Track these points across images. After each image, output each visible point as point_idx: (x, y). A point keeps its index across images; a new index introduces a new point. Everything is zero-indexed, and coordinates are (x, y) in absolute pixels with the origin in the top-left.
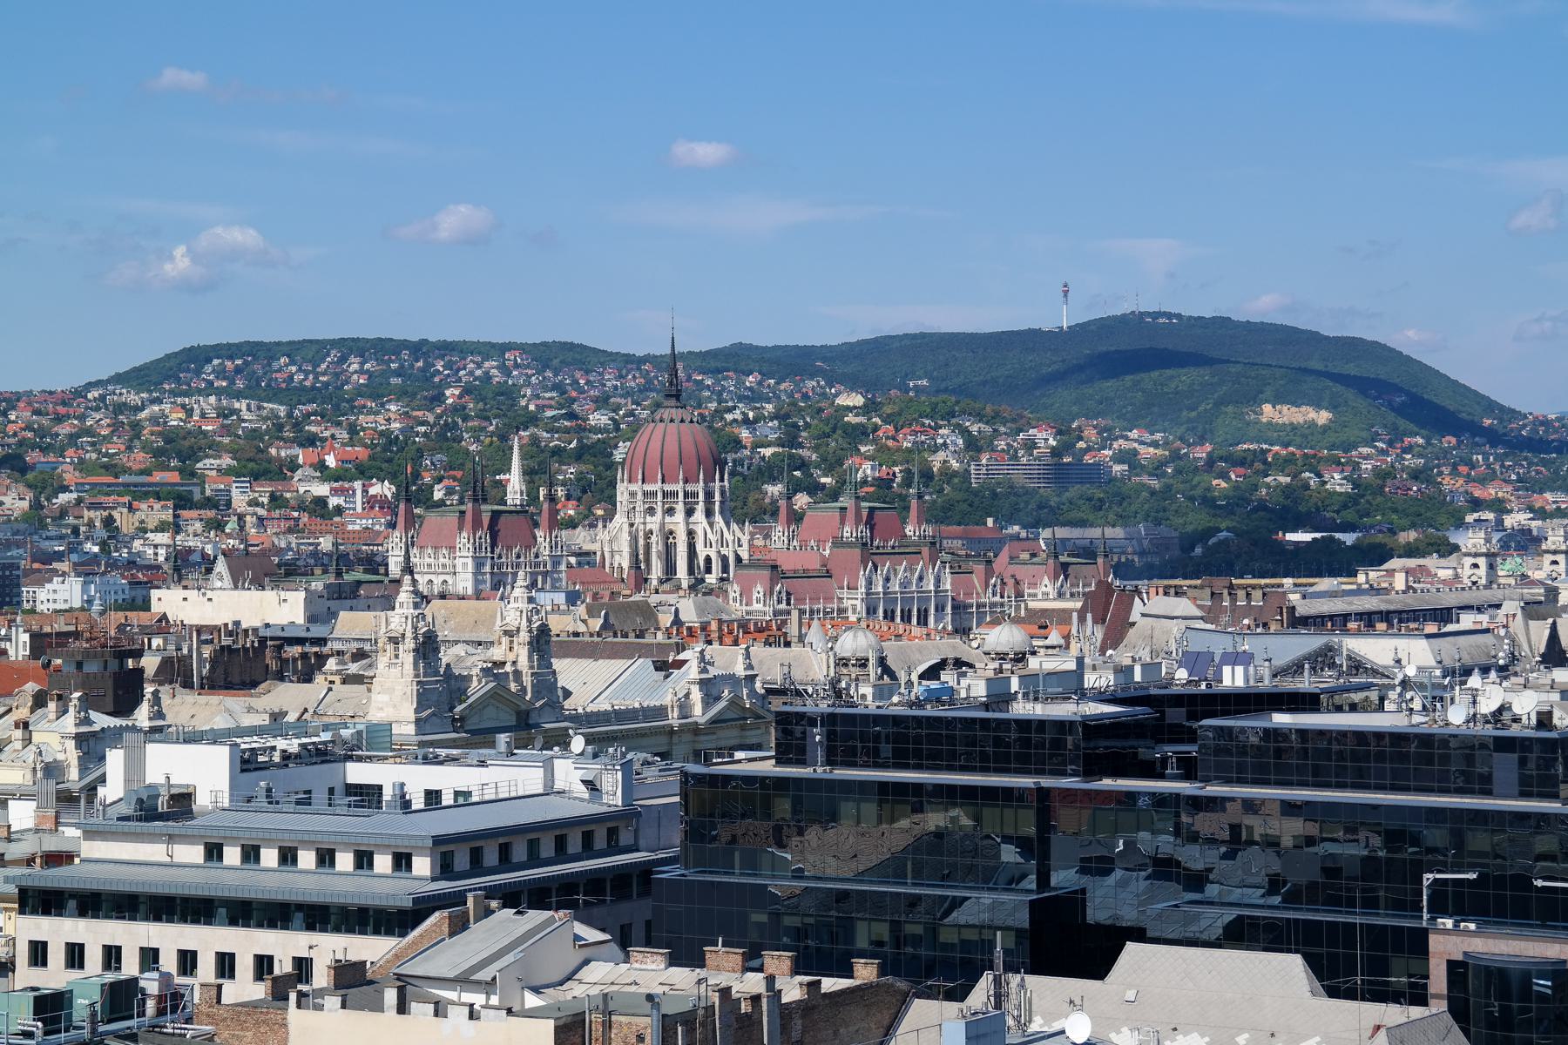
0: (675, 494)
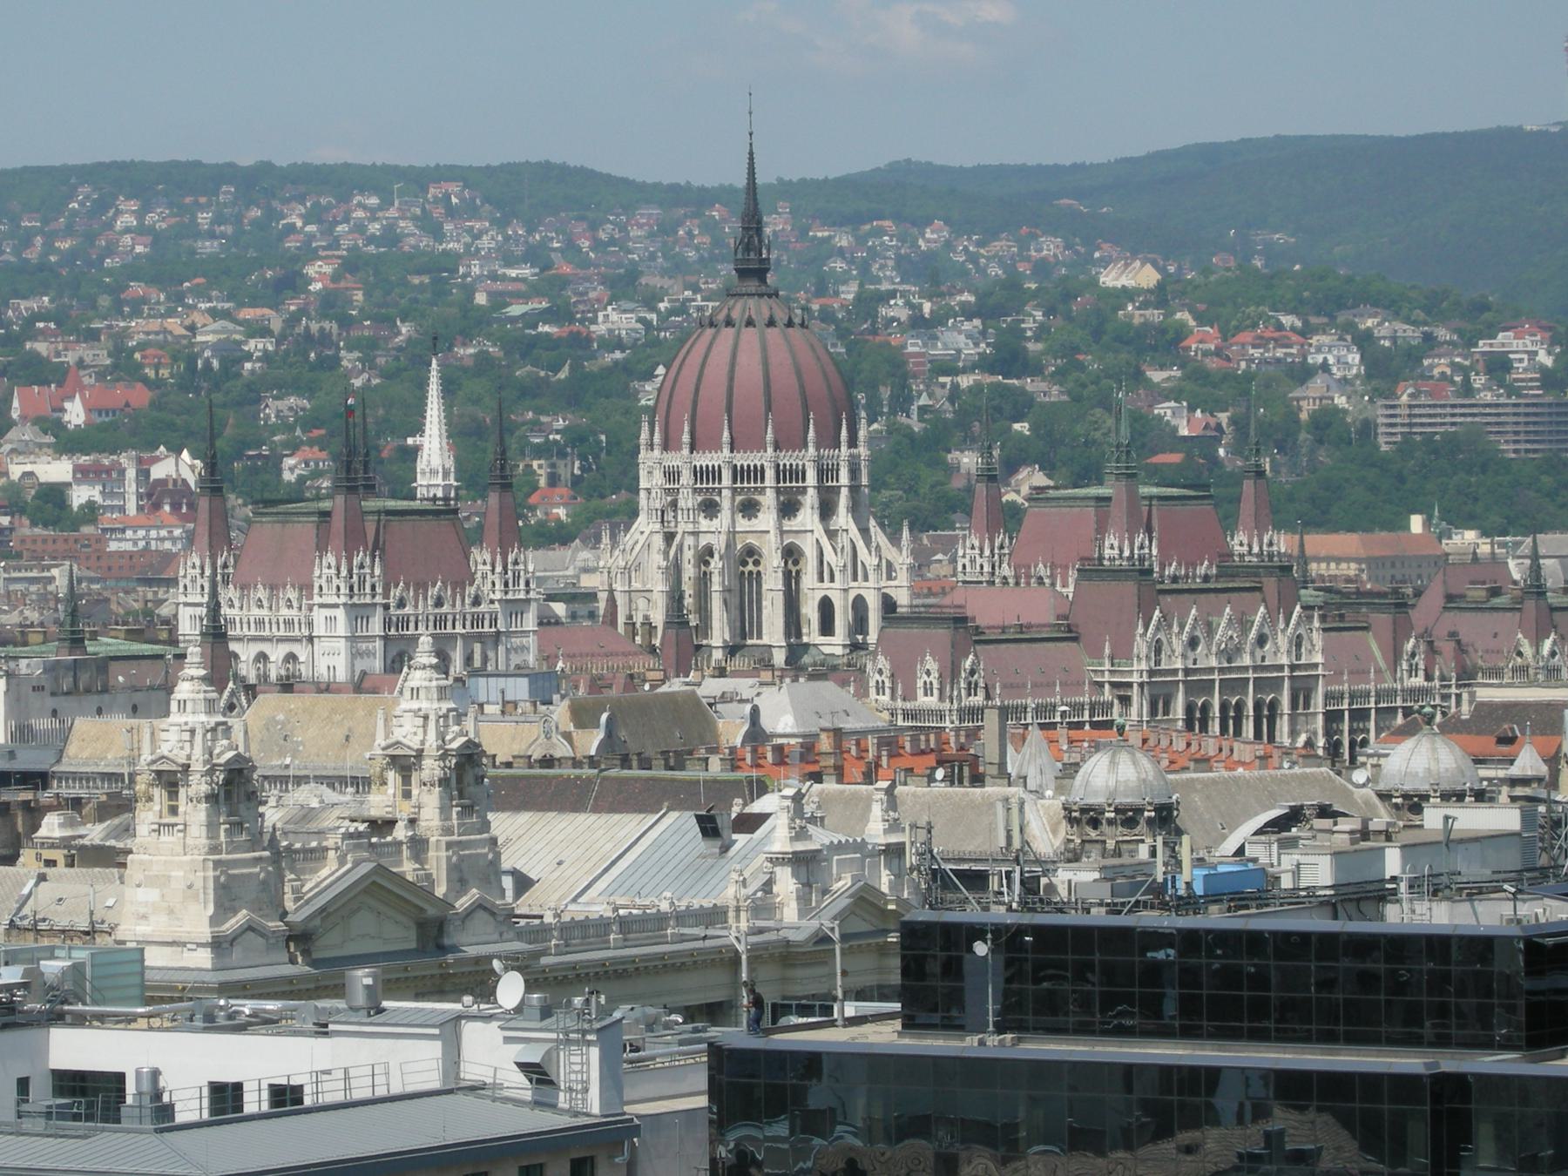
0: (759, 473)
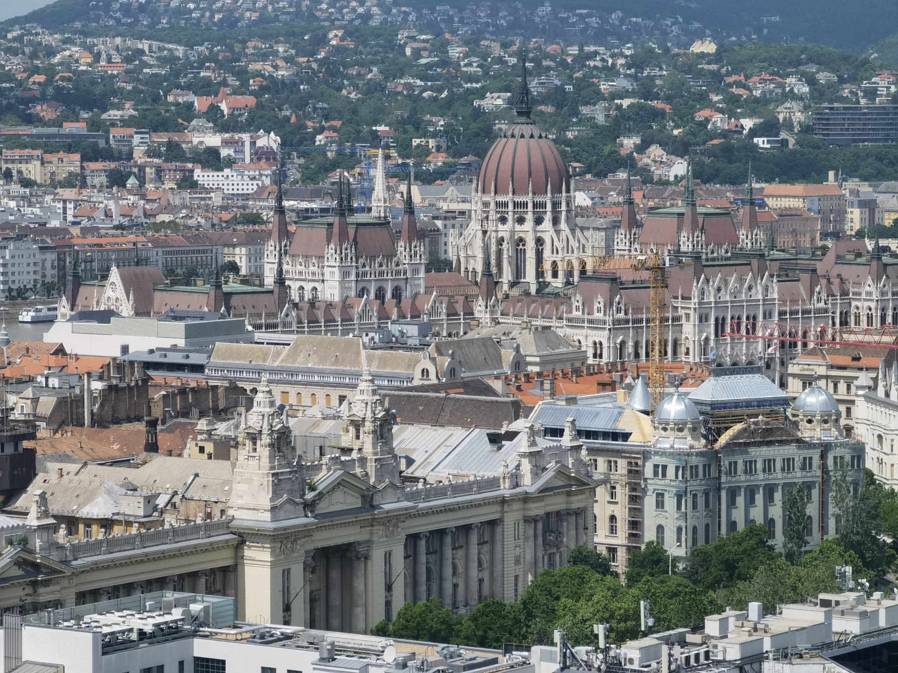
0: (525, 205)
